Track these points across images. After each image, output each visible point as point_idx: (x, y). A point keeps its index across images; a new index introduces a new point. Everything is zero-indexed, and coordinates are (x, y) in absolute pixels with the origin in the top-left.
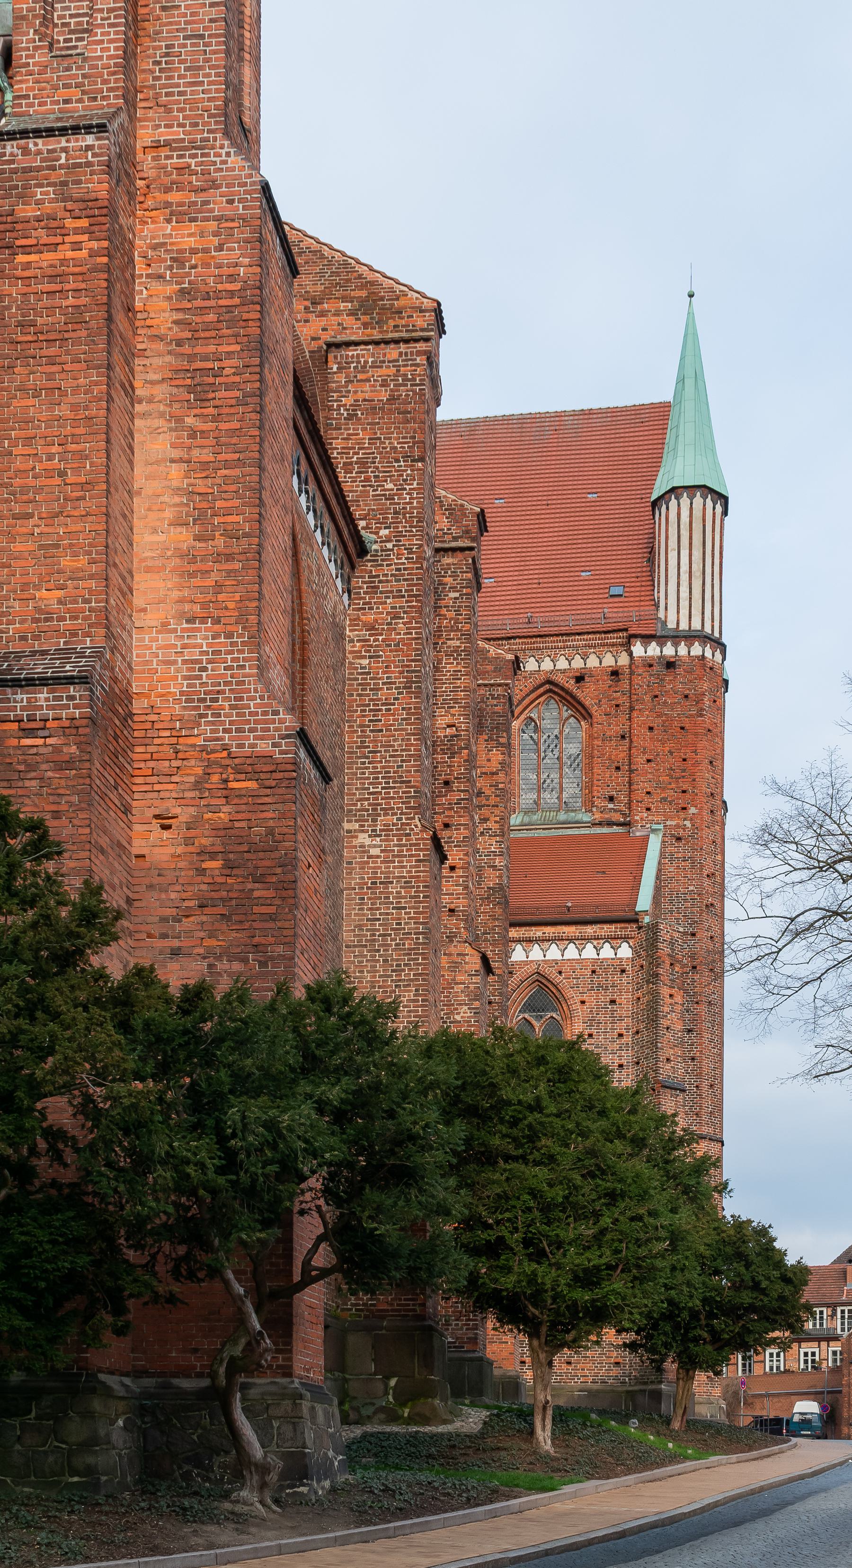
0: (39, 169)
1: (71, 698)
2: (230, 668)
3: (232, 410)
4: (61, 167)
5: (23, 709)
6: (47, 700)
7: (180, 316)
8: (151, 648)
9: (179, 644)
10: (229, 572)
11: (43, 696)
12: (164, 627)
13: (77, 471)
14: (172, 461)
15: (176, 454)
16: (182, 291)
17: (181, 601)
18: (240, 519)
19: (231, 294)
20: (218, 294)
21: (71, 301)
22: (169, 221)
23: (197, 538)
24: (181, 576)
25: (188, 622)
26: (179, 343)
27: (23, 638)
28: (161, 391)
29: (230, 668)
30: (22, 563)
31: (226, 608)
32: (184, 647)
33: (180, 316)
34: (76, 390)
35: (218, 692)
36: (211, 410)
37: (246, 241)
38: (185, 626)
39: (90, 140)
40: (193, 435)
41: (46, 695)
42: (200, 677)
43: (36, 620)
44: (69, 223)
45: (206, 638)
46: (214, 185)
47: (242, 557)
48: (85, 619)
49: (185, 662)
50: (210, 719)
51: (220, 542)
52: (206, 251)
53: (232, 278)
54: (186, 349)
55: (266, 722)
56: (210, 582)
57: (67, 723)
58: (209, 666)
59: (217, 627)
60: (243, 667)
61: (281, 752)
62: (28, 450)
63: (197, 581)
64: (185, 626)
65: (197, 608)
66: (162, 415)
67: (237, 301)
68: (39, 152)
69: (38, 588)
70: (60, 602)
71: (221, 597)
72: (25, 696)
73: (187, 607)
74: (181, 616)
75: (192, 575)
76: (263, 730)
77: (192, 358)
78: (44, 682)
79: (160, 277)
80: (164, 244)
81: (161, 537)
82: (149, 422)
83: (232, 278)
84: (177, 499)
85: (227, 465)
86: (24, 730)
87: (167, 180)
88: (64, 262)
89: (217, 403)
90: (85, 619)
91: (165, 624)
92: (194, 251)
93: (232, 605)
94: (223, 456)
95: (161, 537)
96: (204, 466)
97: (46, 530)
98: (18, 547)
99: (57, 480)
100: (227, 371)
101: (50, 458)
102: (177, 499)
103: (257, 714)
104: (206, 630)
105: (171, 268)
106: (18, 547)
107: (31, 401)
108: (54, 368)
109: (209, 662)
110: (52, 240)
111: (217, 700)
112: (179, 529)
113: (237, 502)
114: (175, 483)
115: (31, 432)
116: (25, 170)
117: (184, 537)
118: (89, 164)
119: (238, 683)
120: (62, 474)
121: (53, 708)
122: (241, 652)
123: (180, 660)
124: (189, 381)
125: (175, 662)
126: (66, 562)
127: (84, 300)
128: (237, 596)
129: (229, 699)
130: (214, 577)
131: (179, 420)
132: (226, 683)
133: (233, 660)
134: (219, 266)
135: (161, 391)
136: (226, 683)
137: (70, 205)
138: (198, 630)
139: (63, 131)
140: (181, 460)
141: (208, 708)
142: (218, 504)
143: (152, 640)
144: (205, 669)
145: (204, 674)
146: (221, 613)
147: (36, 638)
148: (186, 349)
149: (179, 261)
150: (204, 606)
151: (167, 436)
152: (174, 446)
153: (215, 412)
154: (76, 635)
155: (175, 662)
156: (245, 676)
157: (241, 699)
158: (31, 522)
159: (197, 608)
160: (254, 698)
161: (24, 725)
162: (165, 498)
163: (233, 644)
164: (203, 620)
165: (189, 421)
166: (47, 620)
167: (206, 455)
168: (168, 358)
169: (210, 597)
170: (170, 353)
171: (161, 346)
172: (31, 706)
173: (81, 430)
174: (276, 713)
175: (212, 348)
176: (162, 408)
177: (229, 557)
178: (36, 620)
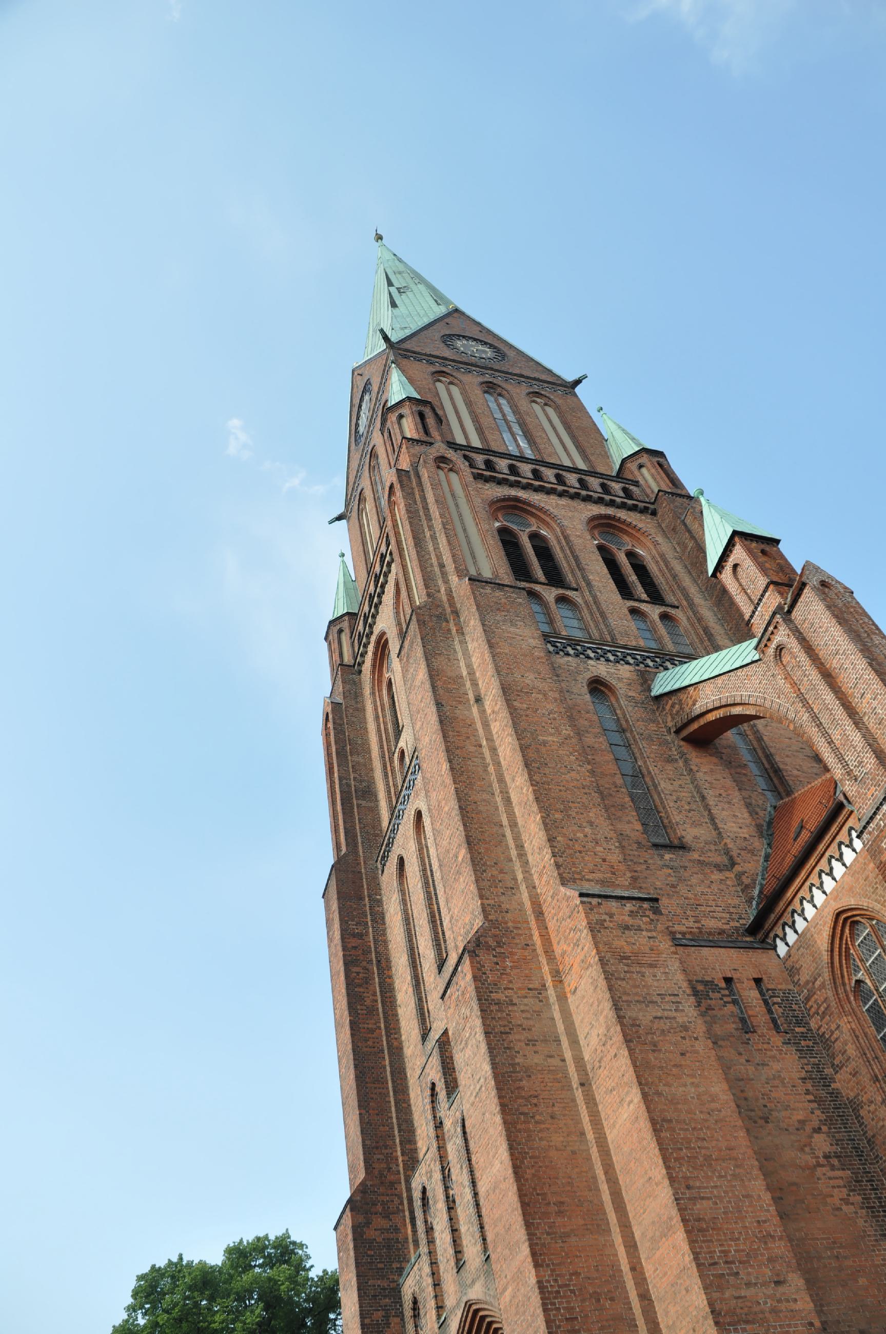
0: (878, 836)
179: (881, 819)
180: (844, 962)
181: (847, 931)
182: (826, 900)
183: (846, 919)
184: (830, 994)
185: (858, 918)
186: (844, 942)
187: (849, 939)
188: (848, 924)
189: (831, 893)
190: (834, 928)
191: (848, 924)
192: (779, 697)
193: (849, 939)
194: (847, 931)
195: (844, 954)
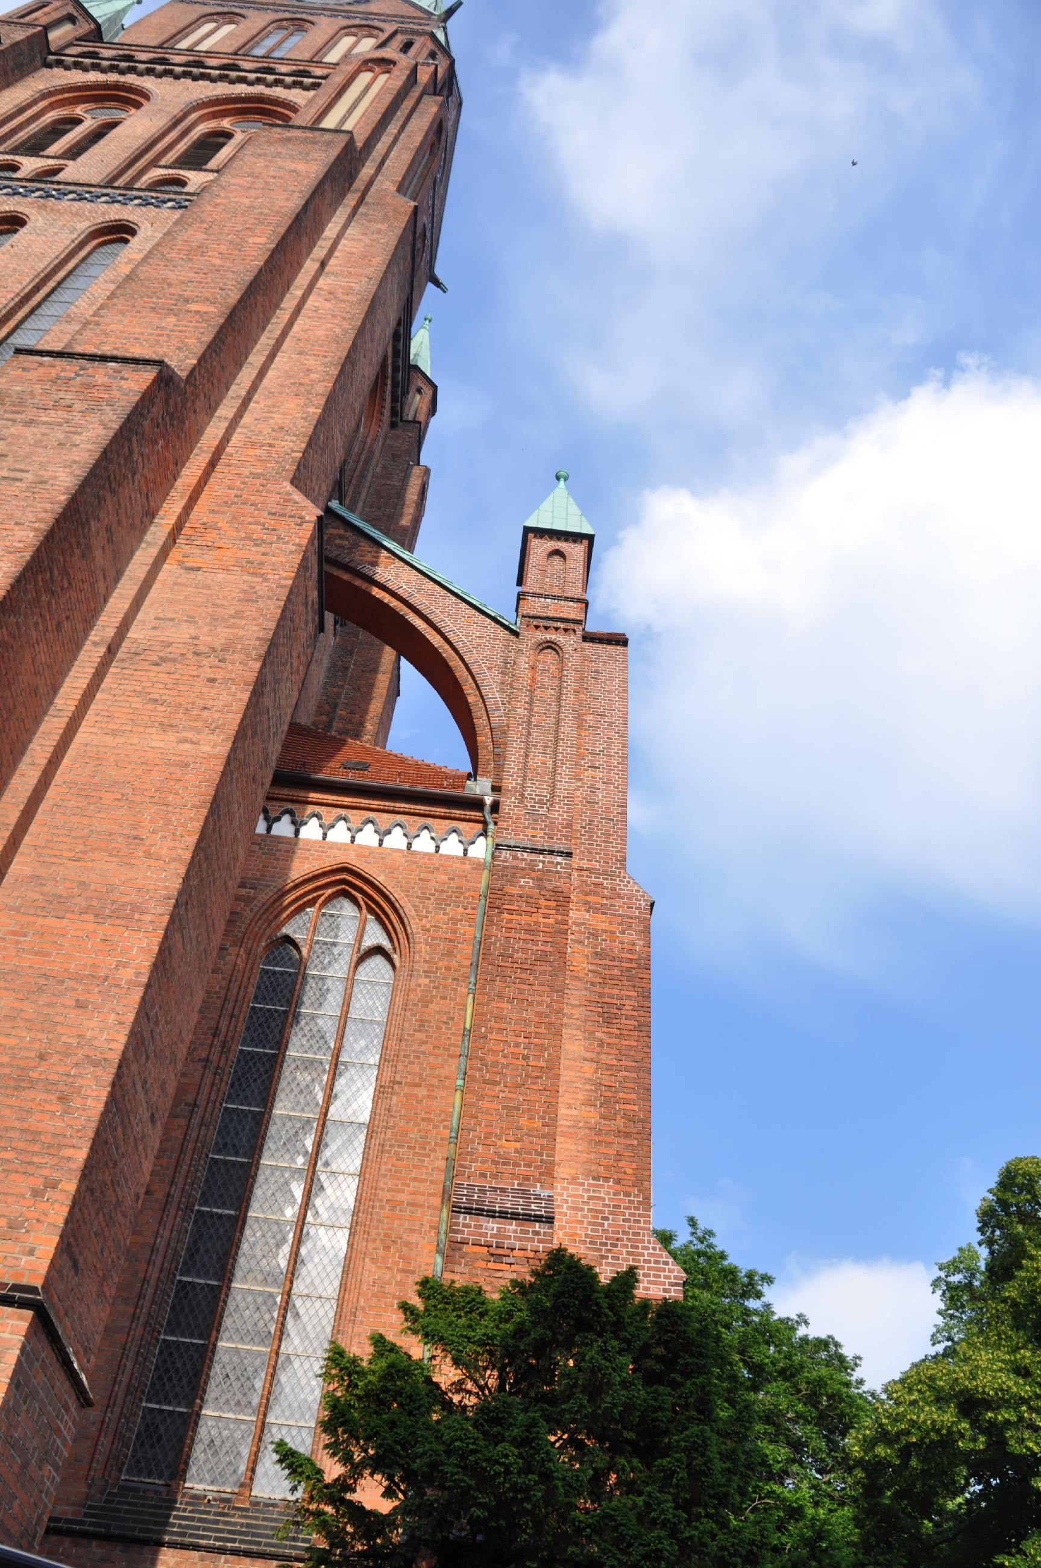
1: (537, 1233)
2: (628, 1221)
4: (539, 870)
5: (492, 1236)
6: (515, 1231)
7: (590, 967)
8: (562, 1195)
9: (586, 1195)
11: (512, 1226)
12: (573, 1180)
14: (585, 1059)
15: (589, 1055)
16: (596, 953)
17: (589, 1161)
18: (636, 1108)
20: (621, 960)
21: (540, 947)
22: (588, 911)
25: (594, 1179)
26: (593, 984)
27: (483, 1175)
29: (628, 1221)
30: (489, 1117)
31: (625, 1173)
32: (590, 1198)
33: (590, 967)
34: (540, 1003)
35: (618, 1239)
36: (615, 1031)
37: (641, 931)
38: (591, 1181)
39: (559, 859)
40: (601, 1044)
44: (542, 902)
45: (608, 1193)
46: (619, 896)
49: (590, 1210)
50: (610, 1261)
51: (620, 1122)
52: (613, 933)
53: (631, 952)
54: (598, 988)
56: (611, 1151)
57: (532, 1255)
58: (611, 1217)
59: (617, 1187)
60: (639, 1222)
62: (499, 1037)
63: (603, 1149)
64: (591, 1181)
66: (579, 1028)
67: (634, 965)
68: (525, 860)
69: (499, 1137)
71: (621, 1164)
72: (496, 1226)
73: (593, 1167)
74: (588, 1174)
76: (655, 1276)
77: (601, 995)
78: (515, 1216)
79: (581, 942)
80: (584, 924)
81: (575, 1112)
82: (569, 1031)
83: (631, 952)
84: (588, 1087)
85: (627, 1069)
86: (492, 1255)
87: (587, 889)
89: (619, 1026)
90: (537, 1167)
92: (604, 931)
93: (630, 1171)
94: (623, 1063)
95: (575, 1112)
96: (609, 1067)
97: (510, 1095)
98: (485, 1104)
100: (627, 1007)
101: (517, 1045)
102: (588, 1087)
104: (609, 1187)
105: (588, 938)
106: (485, 1104)
107: (505, 1005)
108: (524, 987)
109: (610, 1213)
110: (529, 909)
111: (616, 1246)
112: (588, 1109)
113: (634, 1096)
114: (587, 1075)
115: (504, 1026)
116: (513, 867)
117: (593, 1116)
118: (557, 872)
119: (634, 1234)
120: (525, 1058)
121: (520, 1239)
122: (637, 1209)
123: (586, 1208)
124: (600, 1010)
125: (582, 1210)
126: (523, 1121)
127: (549, 948)
128: (634, 1166)
130: (616, 1147)
131: (592, 1033)
132: (624, 1233)
134: (622, 943)
136: (624, 1233)
137: (543, 892)
138: (602, 1186)
139: (541, 852)
140: (592, 1060)
141: (609, 1251)
142: (621, 1095)
143: (564, 1189)
144: (607, 1219)
145: (606, 1223)
146: (621, 1176)
147: (494, 1176)
149: (594, 935)
152: (587, 1050)
153: (618, 1032)
154: (528, 1179)
155: (582, 1210)
156: (640, 1228)
157: (637, 1247)
158: (497, 1088)
161: (493, 1250)
162: (578, 1085)
163: (630, 1202)
164: (606, 1179)
165: (598, 1035)
166: (504, 1164)
168: (584, 993)
169: (612, 1162)
170: (586, 989)
171: (579, 984)
172: (500, 1234)
173: (542, 1030)
175: (617, 991)
176: (578, 1023)
177: (628, 1135)
178: (496, 1163)
179: (543, 862)
180: (292, 908)
181: (330, 891)
182: (346, 844)
183: (344, 881)
184: (248, 914)
185: (359, 896)
186: (315, 895)
187: (323, 898)
188: (339, 888)
189: (360, 846)
190: (325, 874)
191: (339, 888)
192: (489, 668)
193: (323, 898)
194: (330, 891)
195: (301, 902)
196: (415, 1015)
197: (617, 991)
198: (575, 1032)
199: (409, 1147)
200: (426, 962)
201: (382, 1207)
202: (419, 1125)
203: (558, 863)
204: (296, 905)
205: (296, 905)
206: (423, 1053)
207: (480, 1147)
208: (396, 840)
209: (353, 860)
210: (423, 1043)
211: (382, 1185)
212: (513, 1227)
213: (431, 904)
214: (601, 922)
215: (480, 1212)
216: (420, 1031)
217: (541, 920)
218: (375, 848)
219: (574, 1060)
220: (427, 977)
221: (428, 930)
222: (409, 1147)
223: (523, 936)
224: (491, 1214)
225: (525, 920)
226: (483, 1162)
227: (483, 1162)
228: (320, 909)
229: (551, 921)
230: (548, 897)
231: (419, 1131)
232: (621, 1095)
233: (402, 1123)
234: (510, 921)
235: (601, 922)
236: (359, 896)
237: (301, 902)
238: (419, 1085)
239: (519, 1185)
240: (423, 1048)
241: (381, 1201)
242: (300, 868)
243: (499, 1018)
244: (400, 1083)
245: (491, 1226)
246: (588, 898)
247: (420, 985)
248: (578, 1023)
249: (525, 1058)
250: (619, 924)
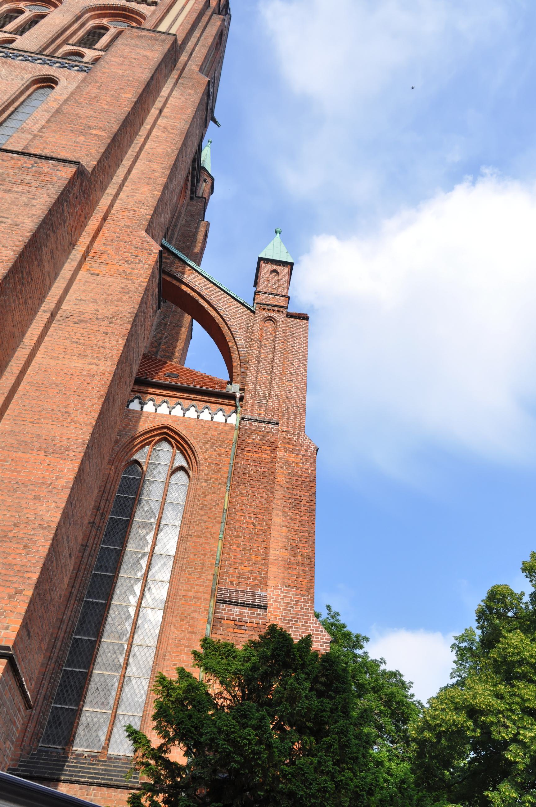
1: (259, 614)
2: (302, 609)
3: (306, 514)
4: (263, 431)
5: (237, 615)
6: (248, 613)
7: (288, 480)
8: (270, 595)
9: (282, 595)
10: (304, 571)
11: (247, 610)
12: (276, 587)
13: (260, 524)
15: (284, 524)
16: (289, 473)
17: (284, 578)
18: (308, 551)
19: (306, 478)
21: (262, 469)
22: (286, 452)
23: (291, 555)
24: (284, 568)
25: (286, 587)
26: (287, 488)
27: (232, 584)
28: (280, 502)
29: (302, 609)
31: (302, 584)
32: (284, 596)
33: (288, 480)
35: (298, 618)
36: (297, 512)
39: (273, 426)
40: (291, 518)
41: (247, 611)
42: (290, 610)
43: (239, 578)
44: (263, 447)
45: (293, 594)
47: (308, 566)
48: (259, 580)
51: (300, 558)
55: (317, 634)
56: (295, 572)
57: (256, 625)
58: (294, 606)
59: (298, 591)
61: (324, 649)
62: (241, 514)
63: (290, 571)
65: (290, 582)
66: (280, 510)
68: (256, 426)
69: (240, 564)
70: (249, 572)
72: (238, 610)
73: (286, 581)
74: (283, 584)
75: (289, 568)
77: (292, 494)
78: (248, 605)
80: (283, 458)
81: (277, 552)
82: (275, 512)
84: (284, 540)
87: (286, 441)
88: (261, 457)
89: (300, 510)
90: (259, 580)
91: (277, 586)
92: (293, 462)
93: (304, 583)
95: (277, 552)
99: (252, 526)
100: (304, 500)
102: (284, 540)
103: (313, 630)
104: (294, 591)
107: (244, 498)
108: (254, 489)
109: (294, 604)
110: (257, 450)
112: (284, 551)
113: (307, 545)
114: (284, 534)
116: (250, 430)
117: (286, 554)
119: (306, 616)
120: (254, 525)
121: (250, 617)
123: (282, 601)
124: (291, 501)
126: (253, 557)
127: (267, 470)
128: (306, 580)
129: (302, 622)
131: (286, 513)
132: (301, 615)
133: (304, 605)
134: (302, 468)
135: (280, 502)
136: (301, 615)
139: (264, 422)
140: (286, 526)
141: (293, 624)
143: (271, 591)
144: (292, 607)
145: (292, 609)
146: (300, 586)
147: (238, 585)
148: (289, 491)
149: (288, 464)
150: (293, 581)
151: (281, 517)
153: (299, 513)
155: (280, 602)
156: (309, 613)
157: (307, 623)
158: (240, 540)
159: (290, 582)
160: (313, 623)
164: (293, 587)
165: (290, 514)
166: (243, 578)
167: (296, 527)
168: (283, 493)
169: (295, 578)
170: (284, 491)
173: (262, 511)
174: (321, 631)
175: (299, 492)
176: (280, 508)
177: (303, 565)
178: (239, 578)
179: (265, 427)
180: (139, 446)
181: (158, 438)
185: (172, 441)
186: (150, 439)
187: (154, 441)
190: (156, 429)
193: (154, 441)
194: (158, 438)
195: (143, 443)
196: (199, 501)
197: (299, 492)
198: (278, 512)
199: (195, 569)
200: (205, 475)
201: (180, 599)
202: (200, 557)
203: (272, 428)
204: (141, 445)
205: (141, 445)
206: (203, 520)
207: (231, 570)
208: (192, 413)
209: (169, 422)
210: (204, 515)
211: (181, 588)
212: (247, 611)
213: (208, 446)
214: (291, 457)
215: (230, 603)
216: (201, 509)
217: (263, 456)
218: (181, 417)
219: (278, 526)
220: (205, 482)
221: (207, 459)
222: (195, 569)
223: (254, 464)
224: (236, 604)
225: (255, 455)
226: (233, 577)
227: (233, 577)
228: (153, 446)
229: (268, 457)
230: (267, 445)
231: (200, 560)
232: (300, 545)
233: (192, 556)
234: (248, 456)
235: (291, 457)
236: (172, 441)
237: (143, 443)
238: (200, 537)
239: (250, 589)
240: (203, 518)
241: (180, 596)
242: (143, 426)
243: (241, 505)
244: (191, 536)
245: (236, 610)
246: (286, 446)
247: (202, 486)
248: (280, 508)
249: (254, 525)
250: (301, 459)
